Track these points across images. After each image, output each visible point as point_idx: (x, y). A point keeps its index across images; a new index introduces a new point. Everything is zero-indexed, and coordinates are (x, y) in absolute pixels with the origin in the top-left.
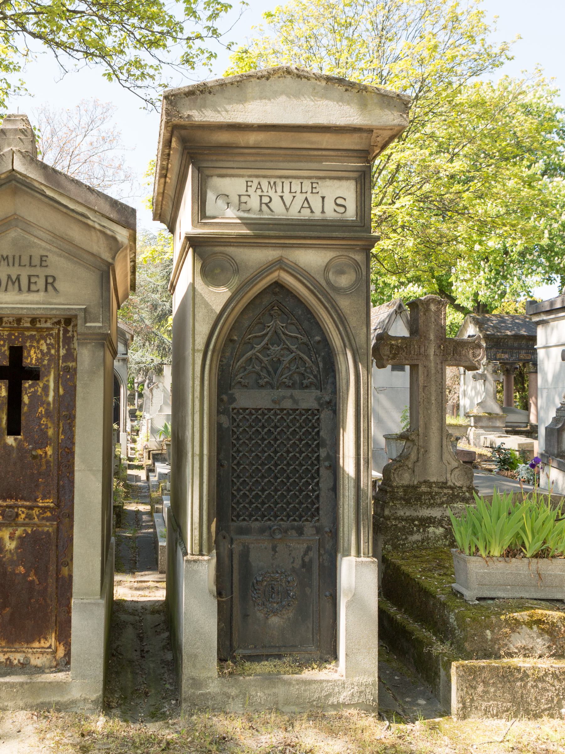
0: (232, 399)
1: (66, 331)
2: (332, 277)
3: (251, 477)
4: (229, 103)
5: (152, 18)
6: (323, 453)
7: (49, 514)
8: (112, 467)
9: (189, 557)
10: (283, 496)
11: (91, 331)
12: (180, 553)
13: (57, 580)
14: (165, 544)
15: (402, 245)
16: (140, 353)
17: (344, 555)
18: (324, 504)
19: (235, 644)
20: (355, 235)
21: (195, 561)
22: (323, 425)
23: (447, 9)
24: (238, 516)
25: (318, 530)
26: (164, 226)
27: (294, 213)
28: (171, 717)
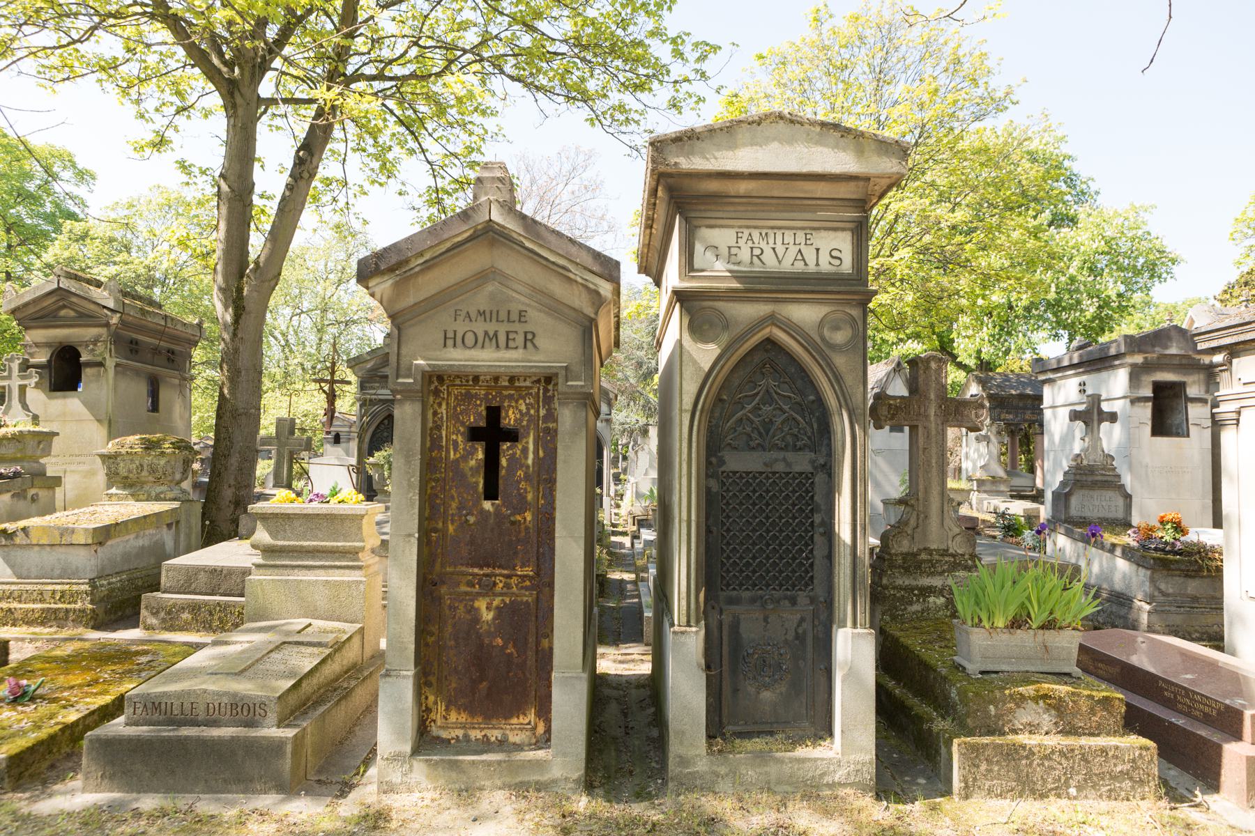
0: (722, 462)
1: (546, 390)
2: (826, 333)
3: (742, 544)
4: (718, 150)
5: (636, 60)
6: (817, 518)
7: (528, 583)
8: (595, 534)
9: (676, 628)
10: (775, 564)
11: (574, 390)
12: (667, 624)
13: (537, 652)
14: (650, 615)
15: (901, 299)
16: (624, 413)
17: (840, 627)
18: (818, 572)
19: (724, 720)
20: (852, 289)
21: (682, 633)
22: (817, 489)
23: (948, 51)
24: (728, 585)
25: (813, 600)
26: (650, 280)
27: (787, 266)
28: (657, 796)
